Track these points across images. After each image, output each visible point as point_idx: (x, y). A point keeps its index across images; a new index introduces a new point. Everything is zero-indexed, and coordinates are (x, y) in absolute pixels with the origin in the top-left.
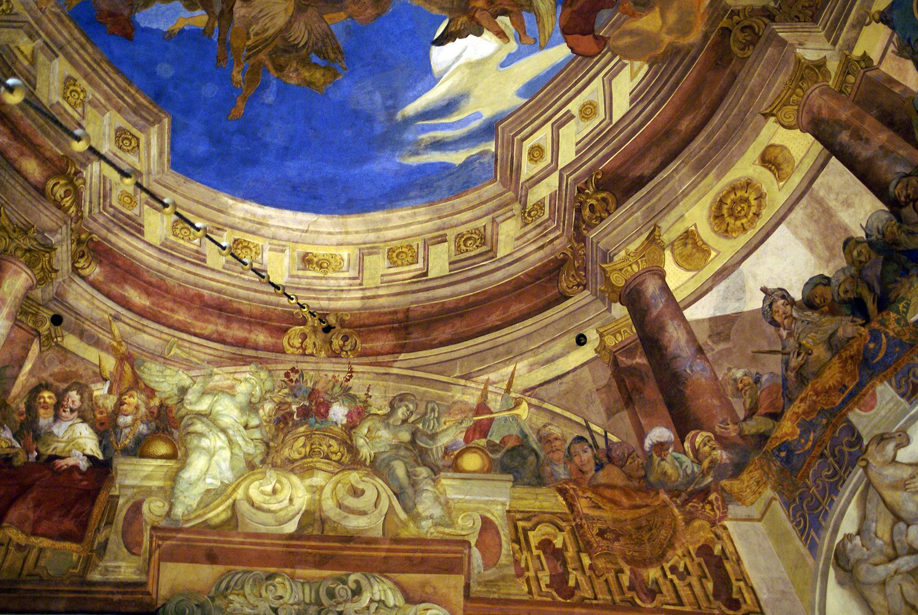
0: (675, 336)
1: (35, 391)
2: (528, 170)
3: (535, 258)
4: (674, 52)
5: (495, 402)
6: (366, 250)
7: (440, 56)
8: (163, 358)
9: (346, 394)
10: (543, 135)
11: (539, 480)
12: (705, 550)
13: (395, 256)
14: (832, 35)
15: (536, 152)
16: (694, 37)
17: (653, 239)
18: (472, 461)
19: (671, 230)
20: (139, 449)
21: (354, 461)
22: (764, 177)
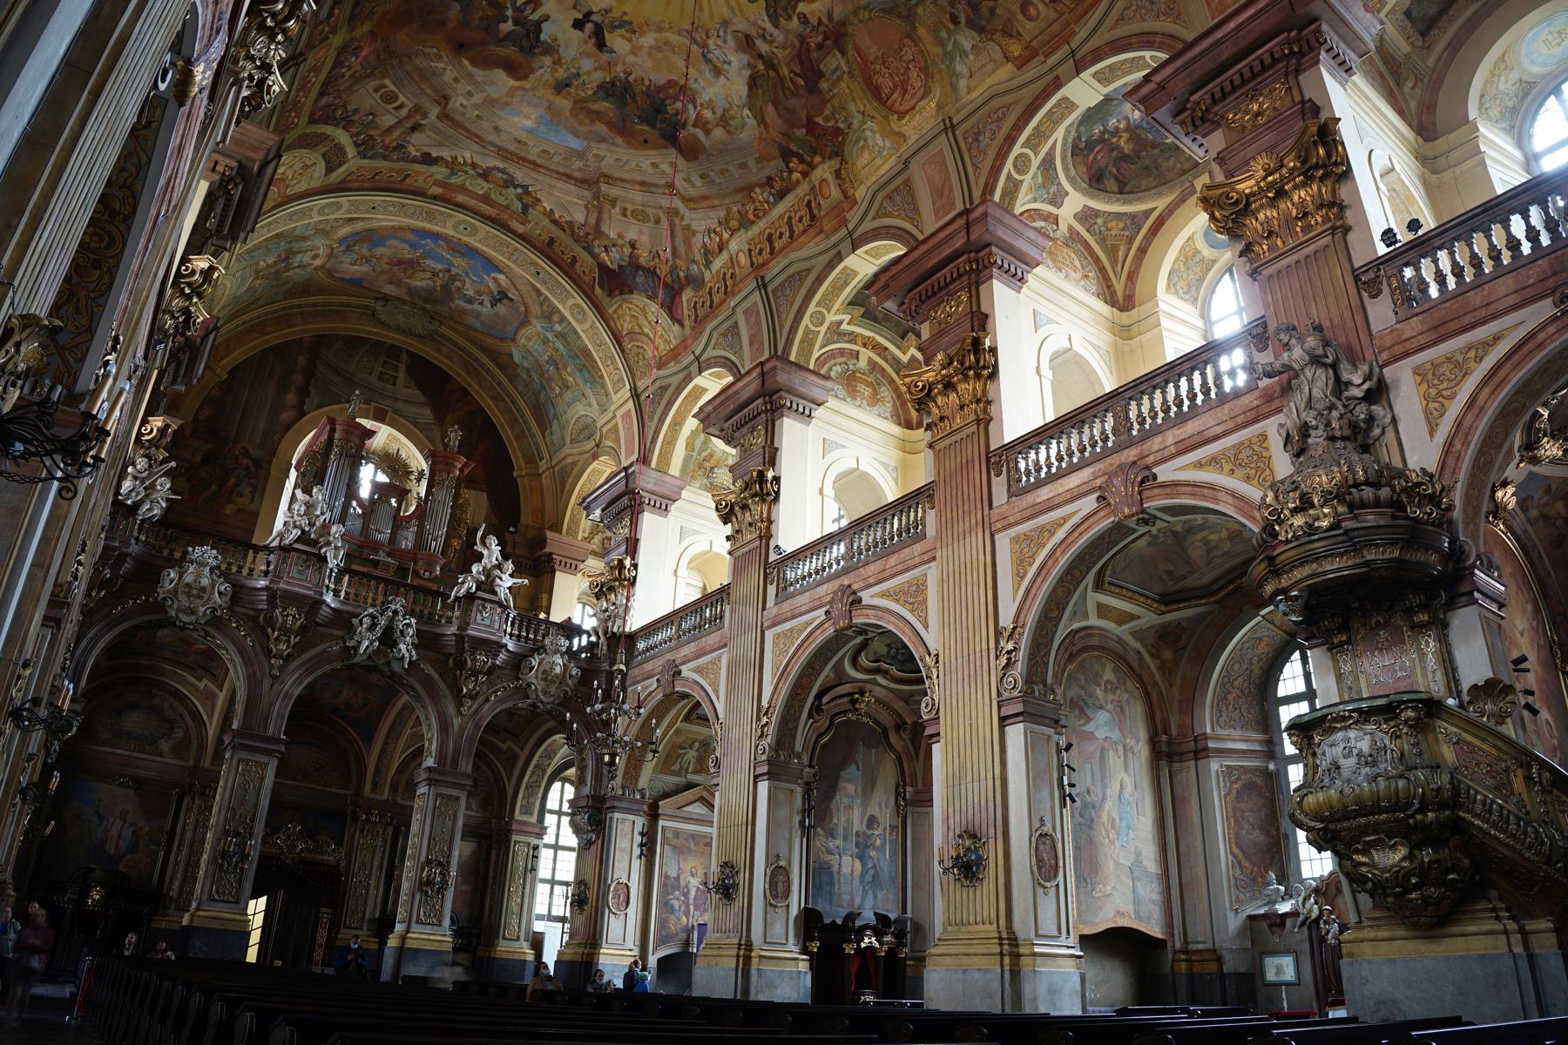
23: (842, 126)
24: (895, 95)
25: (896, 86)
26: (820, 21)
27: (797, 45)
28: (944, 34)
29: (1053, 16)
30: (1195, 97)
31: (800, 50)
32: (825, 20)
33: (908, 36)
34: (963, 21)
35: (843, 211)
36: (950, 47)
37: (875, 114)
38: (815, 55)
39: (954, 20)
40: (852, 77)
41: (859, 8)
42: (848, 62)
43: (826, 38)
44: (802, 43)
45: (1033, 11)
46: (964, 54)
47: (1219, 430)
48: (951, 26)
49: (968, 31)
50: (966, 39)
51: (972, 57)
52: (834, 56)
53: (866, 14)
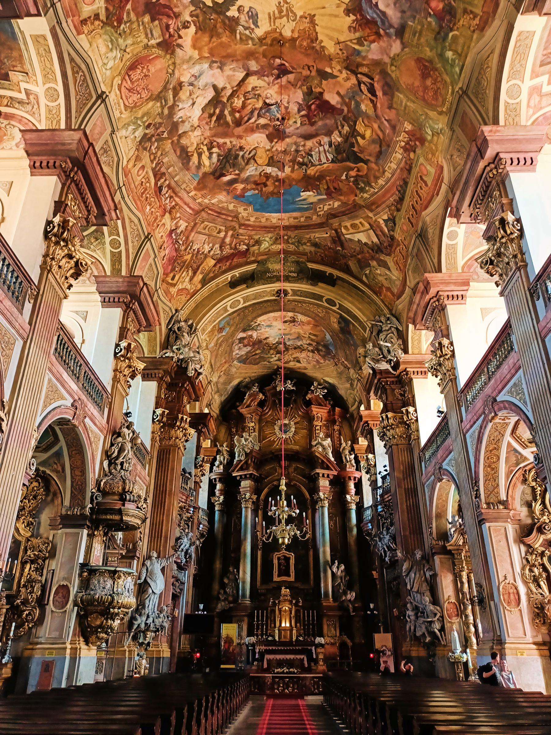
0: (343, 238)
1: (236, 245)
2: (318, 210)
3: (319, 221)
4: (345, 203)
5: (312, 238)
6: (288, 218)
7: (302, 194)
8: (256, 234)
9: (287, 235)
10: (322, 206)
11: (319, 248)
12: (345, 263)
13: (295, 218)
14: (375, 215)
15: (320, 208)
16: (350, 203)
17: (340, 224)
18: (308, 244)
19: (343, 224)
20: (254, 246)
21: (289, 243)
22: (360, 225)
23: (123, 26)
24: (129, 82)
25: (132, 83)
26: (180, 37)
27: (176, 10)
28: (145, 119)
29: (137, 184)
30: (136, 303)
31: (171, 9)
32: (180, 41)
33: (152, 95)
34: (147, 131)
35: (74, 16)
36: (139, 122)
37: (123, 62)
38: (165, 20)
39: (148, 126)
40: (146, 47)
41: (175, 68)
42: (153, 47)
43: (170, 36)
44: (174, 13)
45: (140, 172)
46: (135, 130)
47: (98, 423)
48: (147, 124)
49: (142, 134)
50: (139, 133)
51: (132, 137)
52: (159, 37)
53: (170, 71)
